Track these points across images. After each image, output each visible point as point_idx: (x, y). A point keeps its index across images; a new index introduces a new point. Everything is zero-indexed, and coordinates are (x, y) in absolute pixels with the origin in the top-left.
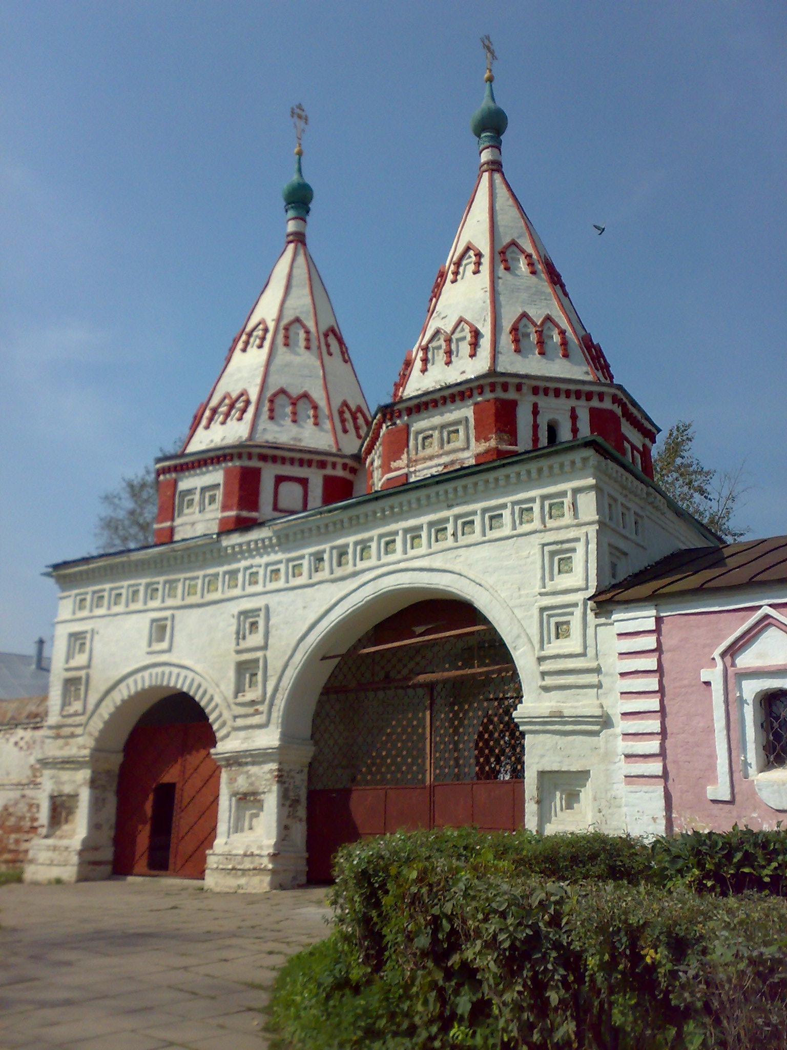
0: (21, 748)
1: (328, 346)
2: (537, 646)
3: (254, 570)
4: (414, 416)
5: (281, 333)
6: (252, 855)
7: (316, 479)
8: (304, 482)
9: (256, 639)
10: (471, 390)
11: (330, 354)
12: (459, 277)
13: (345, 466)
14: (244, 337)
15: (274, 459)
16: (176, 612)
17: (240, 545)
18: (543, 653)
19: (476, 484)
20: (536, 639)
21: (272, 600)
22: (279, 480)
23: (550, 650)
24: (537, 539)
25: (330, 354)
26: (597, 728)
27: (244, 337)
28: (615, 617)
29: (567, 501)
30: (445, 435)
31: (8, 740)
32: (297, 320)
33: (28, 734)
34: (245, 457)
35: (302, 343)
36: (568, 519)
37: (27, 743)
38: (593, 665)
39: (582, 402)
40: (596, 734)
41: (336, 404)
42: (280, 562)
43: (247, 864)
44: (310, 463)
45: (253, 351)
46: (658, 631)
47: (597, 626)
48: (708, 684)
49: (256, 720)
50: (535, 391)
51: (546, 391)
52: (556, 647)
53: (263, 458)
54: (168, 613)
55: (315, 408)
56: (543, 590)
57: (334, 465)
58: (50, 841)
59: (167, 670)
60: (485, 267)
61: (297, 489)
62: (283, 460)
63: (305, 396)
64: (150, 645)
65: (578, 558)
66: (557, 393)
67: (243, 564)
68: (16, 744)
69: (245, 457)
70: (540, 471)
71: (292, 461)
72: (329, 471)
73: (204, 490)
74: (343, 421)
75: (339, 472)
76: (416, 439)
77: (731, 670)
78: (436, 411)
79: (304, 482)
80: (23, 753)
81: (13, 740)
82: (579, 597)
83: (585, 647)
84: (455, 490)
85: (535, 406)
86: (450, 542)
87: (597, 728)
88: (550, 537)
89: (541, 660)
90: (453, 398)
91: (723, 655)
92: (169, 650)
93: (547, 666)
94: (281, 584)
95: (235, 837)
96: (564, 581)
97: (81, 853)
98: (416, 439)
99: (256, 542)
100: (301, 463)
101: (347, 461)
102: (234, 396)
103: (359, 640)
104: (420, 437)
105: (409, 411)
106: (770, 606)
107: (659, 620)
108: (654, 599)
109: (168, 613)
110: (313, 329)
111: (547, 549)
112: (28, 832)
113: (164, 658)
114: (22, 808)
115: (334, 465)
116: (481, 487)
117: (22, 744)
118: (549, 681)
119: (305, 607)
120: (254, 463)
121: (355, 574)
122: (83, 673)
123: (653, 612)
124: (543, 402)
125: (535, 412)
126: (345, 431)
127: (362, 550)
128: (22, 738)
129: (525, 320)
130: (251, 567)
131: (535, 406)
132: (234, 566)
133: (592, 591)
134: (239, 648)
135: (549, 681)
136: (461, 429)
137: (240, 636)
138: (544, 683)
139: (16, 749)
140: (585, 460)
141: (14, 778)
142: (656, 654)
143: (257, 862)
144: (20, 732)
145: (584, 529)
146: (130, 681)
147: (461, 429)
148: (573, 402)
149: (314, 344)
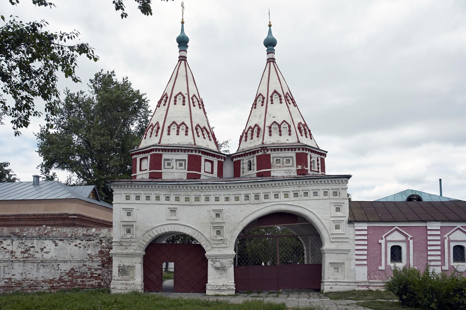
0: (80, 247)
3: (218, 196)
4: (273, 152)
22: (206, 160)
30: (285, 160)
31: (70, 244)
33: (84, 242)
37: (83, 245)
39: (320, 156)
67: (212, 193)
76: (273, 160)
78: (282, 152)
81: (74, 243)
98: (273, 160)
104: (275, 159)
112: (90, 278)
113: (176, 222)
114: (84, 269)
117: (80, 246)
119: (241, 211)
128: (80, 244)
131: (311, 155)
132: (207, 193)
141: (77, 257)
146: (157, 229)
148: (318, 155)
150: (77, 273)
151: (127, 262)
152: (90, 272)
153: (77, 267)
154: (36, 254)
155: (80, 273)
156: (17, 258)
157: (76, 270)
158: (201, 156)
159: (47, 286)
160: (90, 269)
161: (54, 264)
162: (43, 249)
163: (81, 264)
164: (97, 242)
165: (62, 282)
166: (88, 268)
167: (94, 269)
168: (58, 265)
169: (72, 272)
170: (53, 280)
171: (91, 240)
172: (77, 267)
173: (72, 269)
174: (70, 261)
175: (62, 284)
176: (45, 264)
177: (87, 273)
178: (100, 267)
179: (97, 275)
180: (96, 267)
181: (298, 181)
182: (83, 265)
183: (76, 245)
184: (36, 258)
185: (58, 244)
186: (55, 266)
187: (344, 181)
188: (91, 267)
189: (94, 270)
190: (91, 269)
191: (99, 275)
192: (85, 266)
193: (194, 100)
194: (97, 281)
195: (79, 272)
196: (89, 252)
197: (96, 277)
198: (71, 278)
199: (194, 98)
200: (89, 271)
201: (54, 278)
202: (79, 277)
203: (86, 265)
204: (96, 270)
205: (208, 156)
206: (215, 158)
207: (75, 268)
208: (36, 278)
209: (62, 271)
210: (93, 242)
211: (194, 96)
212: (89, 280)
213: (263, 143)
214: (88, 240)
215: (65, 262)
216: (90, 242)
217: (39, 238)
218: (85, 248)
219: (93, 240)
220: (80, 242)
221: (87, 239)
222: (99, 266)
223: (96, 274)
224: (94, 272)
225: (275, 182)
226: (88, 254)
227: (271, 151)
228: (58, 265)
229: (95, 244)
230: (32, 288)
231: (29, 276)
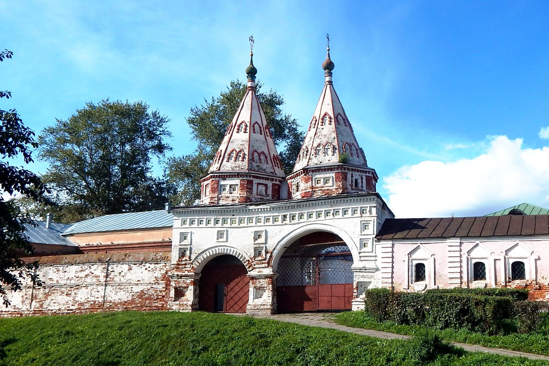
0: (149, 271)
1: (267, 133)
2: (359, 249)
3: (260, 218)
4: (314, 173)
5: (252, 127)
6: (264, 305)
7: (270, 184)
8: (266, 185)
9: (262, 240)
10: (334, 168)
11: (268, 136)
12: (324, 124)
13: (279, 181)
14: (236, 127)
15: (257, 177)
16: (228, 229)
17: (255, 209)
18: (360, 251)
19: (341, 201)
20: (359, 247)
21: (268, 228)
23: (363, 250)
24: (359, 219)
25: (268, 136)
26: (375, 271)
27: (236, 127)
28: (381, 242)
29: (368, 209)
32: (257, 123)
33: (153, 266)
34: (248, 176)
35: (259, 132)
36: (368, 214)
37: (152, 269)
38: (375, 255)
40: (374, 272)
41: (272, 156)
42: (270, 216)
43: (262, 307)
44: (268, 179)
45: (241, 133)
46: (393, 247)
47: (376, 245)
48: (404, 261)
49: (263, 265)
50: (352, 170)
51: (355, 170)
52: (364, 249)
53: (254, 177)
54: (225, 229)
55: (266, 157)
56: (361, 234)
57: (276, 180)
58: (177, 302)
59: (226, 248)
60: (333, 123)
61: (264, 188)
62: (260, 178)
63: (263, 153)
64: (218, 239)
65: (371, 226)
66: (358, 171)
68: (146, 269)
69: (248, 176)
70: (360, 199)
71: (263, 178)
72: (274, 182)
73: (231, 186)
74: (275, 162)
75: (277, 183)
76: (315, 180)
77: (410, 258)
78: (323, 173)
79: (266, 185)
80: (150, 272)
82: (371, 237)
83: (373, 250)
84: (334, 201)
85: (352, 174)
86: (332, 217)
87: (375, 271)
88: (363, 219)
89: (360, 253)
90: (328, 170)
91: (408, 254)
92: (227, 241)
93: (362, 255)
94: (271, 223)
95: (256, 300)
96: (366, 232)
97: (192, 306)
99: (261, 209)
100: (266, 179)
101: (280, 179)
102: (238, 150)
103: (294, 242)
105: (313, 171)
106: (420, 243)
107: (393, 245)
108: (392, 239)
109: (225, 229)
110: (261, 126)
111: (362, 222)
114: (152, 292)
115: (276, 180)
116: (342, 201)
117: (149, 269)
118: (362, 259)
119: (280, 232)
120: (251, 179)
121: (299, 223)
122: (189, 247)
123: (391, 243)
124: (355, 173)
125: (352, 177)
126: (275, 166)
127: (301, 216)
128: (149, 267)
129: (347, 144)
130: (259, 217)
133: (374, 236)
134: (255, 243)
135: (362, 259)
136: (331, 180)
137: (255, 239)
138: (360, 259)
139: (147, 271)
140: (374, 198)
142: (391, 253)
143: (266, 307)
144: (148, 265)
145: (373, 218)
147: (331, 180)
149: (263, 132)
150: (146, 295)
151: (182, 283)
152: (156, 294)
153: (146, 290)
154: (115, 277)
155: (148, 295)
156: (100, 282)
157: (145, 292)
158: (253, 180)
159: (122, 308)
160: (156, 291)
161: (128, 287)
162: (121, 273)
163: (149, 287)
164: (163, 266)
165: (134, 304)
166: (154, 290)
167: (160, 291)
168: (132, 288)
169: (141, 295)
170: (127, 302)
171: (158, 264)
172: (146, 290)
173: (142, 291)
174: (141, 284)
175: (133, 306)
176: (122, 287)
177: (153, 295)
178: (164, 289)
179: (161, 297)
180: (161, 289)
181: (329, 201)
182: (151, 288)
183: (146, 269)
184: (115, 281)
185: (133, 268)
186: (129, 289)
187: (372, 198)
188: (158, 289)
189: (159, 292)
190: (157, 291)
191: (163, 297)
192: (152, 289)
193: (339, 118)
194: (161, 303)
195: (148, 294)
196: (156, 275)
197: (160, 298)
198: (141, 300)
199: (256, 125)
200: (155, 293)
201: (128, 300)
202: (147, 299)
203: (153, 287)
204: (161, 291)
205: (261, 180)
206: (269, 181)
207: (144, 290)
208: (114, 300)
209: (134, 294)
210: (159, 265)
211: (339, 114)
212: (155, 302)
213: (308, 165)
214: (155, 264)
215: (137, 284)
216: (157, 265)
217: (117, 263)
218: (153, 271)
219: (160, 264)
220: (149, 265)
221: (155, 263)
222: (163, 288)
223: (160, 296)
224: (160, 294)
225: (309, 202)
226: (155, 277)
227: (312, 172)
228: (132, 288)
229: (161, 268)
230: (111, 309)
231: (109, 299)
